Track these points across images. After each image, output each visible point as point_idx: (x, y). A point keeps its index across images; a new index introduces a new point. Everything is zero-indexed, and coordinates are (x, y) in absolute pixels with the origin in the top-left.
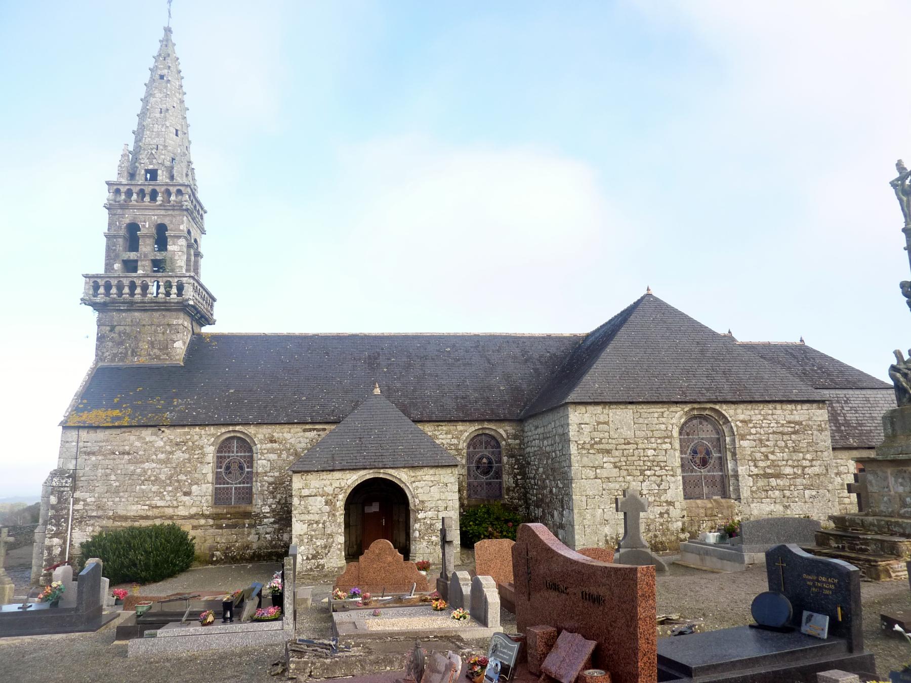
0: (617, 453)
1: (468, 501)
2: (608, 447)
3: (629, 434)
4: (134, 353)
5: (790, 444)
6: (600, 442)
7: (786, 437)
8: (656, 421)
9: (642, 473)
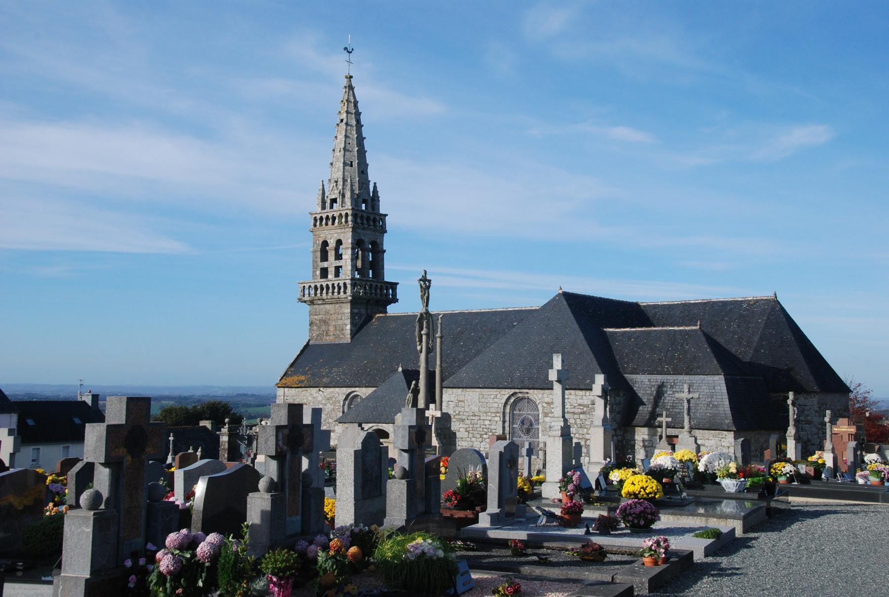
0: (468, 422)
1: (767, 441)
2: (464, 417)
3: (476, 409)
4: (327, 335)
5: (578, 421)
6: (459, 414)
7: (576, 416)
8: (491, 401)
9: (481, 436)
